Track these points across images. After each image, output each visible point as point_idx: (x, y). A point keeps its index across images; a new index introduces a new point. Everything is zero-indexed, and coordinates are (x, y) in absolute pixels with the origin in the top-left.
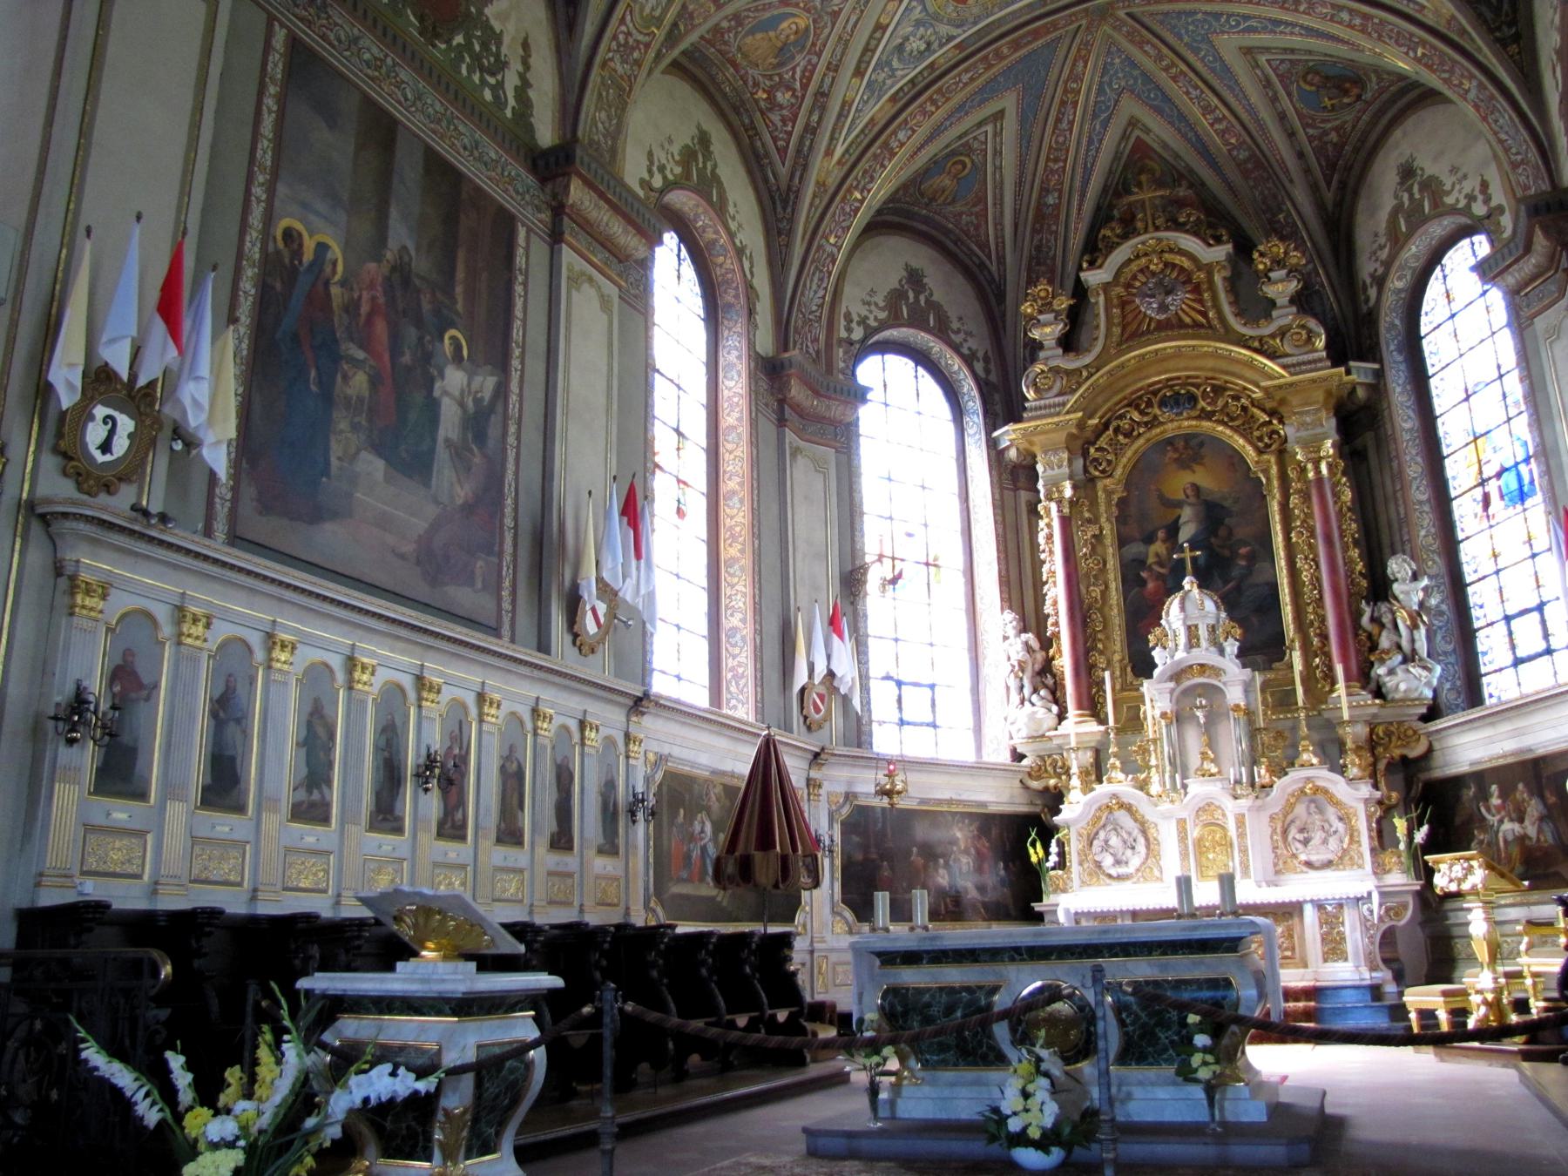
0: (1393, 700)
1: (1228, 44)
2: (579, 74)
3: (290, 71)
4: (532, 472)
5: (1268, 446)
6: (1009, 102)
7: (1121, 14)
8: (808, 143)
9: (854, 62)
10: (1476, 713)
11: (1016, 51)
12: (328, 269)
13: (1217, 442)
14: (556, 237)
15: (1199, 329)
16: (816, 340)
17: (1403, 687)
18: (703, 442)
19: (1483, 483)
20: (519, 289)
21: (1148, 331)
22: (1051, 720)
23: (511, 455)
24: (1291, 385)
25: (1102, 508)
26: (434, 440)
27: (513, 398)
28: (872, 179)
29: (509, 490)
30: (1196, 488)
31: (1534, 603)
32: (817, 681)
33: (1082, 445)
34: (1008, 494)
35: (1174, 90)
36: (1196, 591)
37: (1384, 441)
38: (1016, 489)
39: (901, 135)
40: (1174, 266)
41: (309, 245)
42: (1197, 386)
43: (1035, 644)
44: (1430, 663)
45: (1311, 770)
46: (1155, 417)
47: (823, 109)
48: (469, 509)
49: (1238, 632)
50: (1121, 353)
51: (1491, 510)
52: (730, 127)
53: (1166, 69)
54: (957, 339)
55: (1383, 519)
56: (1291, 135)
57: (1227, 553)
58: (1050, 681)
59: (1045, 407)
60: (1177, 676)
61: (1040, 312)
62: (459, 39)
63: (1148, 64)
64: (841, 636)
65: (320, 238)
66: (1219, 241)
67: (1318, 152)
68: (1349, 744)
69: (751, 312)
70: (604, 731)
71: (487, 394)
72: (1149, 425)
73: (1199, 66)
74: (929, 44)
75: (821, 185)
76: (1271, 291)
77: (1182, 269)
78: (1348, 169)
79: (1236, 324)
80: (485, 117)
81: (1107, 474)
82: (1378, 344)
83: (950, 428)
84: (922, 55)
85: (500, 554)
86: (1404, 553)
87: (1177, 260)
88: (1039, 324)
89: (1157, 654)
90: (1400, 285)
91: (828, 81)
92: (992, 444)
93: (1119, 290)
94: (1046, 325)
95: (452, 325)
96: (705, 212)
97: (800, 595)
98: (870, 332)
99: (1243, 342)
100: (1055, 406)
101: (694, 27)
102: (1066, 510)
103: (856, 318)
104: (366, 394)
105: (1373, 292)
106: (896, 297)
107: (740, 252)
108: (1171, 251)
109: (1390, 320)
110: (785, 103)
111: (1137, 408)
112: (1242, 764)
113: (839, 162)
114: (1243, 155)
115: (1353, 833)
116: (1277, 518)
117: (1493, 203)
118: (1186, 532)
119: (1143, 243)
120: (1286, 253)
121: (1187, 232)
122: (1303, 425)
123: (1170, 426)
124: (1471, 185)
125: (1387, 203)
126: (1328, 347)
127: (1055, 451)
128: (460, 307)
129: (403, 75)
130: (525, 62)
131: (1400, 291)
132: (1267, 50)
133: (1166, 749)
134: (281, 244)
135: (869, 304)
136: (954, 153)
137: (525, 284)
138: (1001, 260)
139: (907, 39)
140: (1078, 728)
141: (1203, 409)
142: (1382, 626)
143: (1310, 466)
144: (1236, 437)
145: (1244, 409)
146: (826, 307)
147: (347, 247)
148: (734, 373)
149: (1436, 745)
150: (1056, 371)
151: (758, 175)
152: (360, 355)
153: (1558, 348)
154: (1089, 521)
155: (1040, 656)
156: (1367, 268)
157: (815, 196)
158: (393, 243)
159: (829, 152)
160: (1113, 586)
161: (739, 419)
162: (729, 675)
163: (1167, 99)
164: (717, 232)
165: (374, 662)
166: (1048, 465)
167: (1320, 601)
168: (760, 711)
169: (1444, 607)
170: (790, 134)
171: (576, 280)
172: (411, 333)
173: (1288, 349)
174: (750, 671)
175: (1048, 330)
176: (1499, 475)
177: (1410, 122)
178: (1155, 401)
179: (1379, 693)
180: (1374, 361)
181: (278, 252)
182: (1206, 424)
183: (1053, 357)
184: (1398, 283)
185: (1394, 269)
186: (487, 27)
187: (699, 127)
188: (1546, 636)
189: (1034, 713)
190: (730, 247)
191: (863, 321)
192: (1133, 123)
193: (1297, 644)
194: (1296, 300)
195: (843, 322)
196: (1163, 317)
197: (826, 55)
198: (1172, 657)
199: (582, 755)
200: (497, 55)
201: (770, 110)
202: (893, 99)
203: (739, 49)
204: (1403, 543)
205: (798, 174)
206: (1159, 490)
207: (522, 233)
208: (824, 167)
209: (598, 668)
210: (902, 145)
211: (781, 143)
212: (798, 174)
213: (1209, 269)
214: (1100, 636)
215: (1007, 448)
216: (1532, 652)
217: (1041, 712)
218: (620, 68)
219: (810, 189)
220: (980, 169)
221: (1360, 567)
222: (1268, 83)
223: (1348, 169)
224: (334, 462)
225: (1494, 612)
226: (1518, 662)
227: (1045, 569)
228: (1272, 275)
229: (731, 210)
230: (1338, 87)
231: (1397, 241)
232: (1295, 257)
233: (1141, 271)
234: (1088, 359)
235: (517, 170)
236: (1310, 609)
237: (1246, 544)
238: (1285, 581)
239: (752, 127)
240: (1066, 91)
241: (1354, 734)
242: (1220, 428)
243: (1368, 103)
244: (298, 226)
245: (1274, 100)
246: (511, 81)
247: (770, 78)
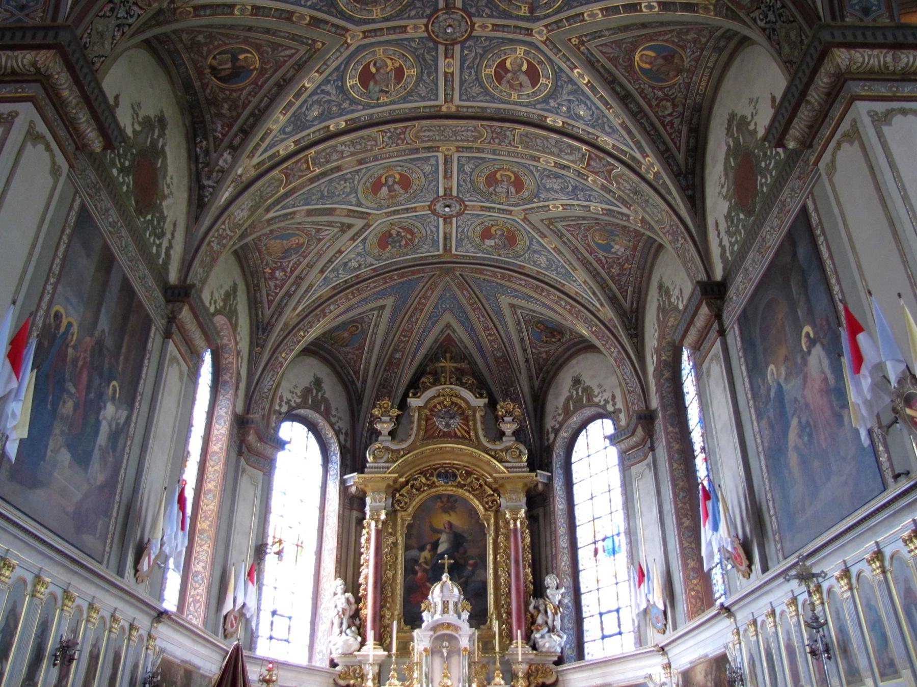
0: (541, 652)
1: (505, 301)
2: (196, 243)
3: (77, 223)
4: (132, 472)
5: (490, 507)
6: (389, 302)
7: (457, 274)
8: (285, 301)
9: (321, 267)
10: (581, 663)
11: (401, 278)
12: (70, 337)
13: (465, 501)
14: (167, 335)
15: (463, 439)
16: (263, 409)
17: (547, 645)
18: (198, 459)
19: (595, 543)
20: (146, 361)
21: (438, 436)
22: (357, 646)
23: (126, 457)
24: (508, 478)
25: (399, 528)
26: (94, 447)
27: (132, 425)
28: (311, 327)
29: (121, 478)
30: (451, 525)
31: (615, 608)
32: (237, 609)
33: (393, 490)
34: (347, 512)
35: (472, 315)
36: (449, 582)
37: (549, 514)
38: (351, 509)
39: (332, 307)
40: (457, 404)
41: (65, 322)
42: (458, 470)
43: (352, 600)
44: (561, 633)
46: (434, 482)
47: (299, 285)
48: (102, 488)
49: (469, 607)
50: (422, 446)
51: (598, 556)
52: (247, 285)
53: (471, 305)
54: (333, 420)
55: (543, 556)
56: (525, 350)
57: (462, 562)
58: (357, 622)
59: (378, 468)
60: (434, 628)
61: (382, 415)
62: (149, 217)
63: (464, 301)
64: (253, 583)
65: (70, 319)
66: (481, 396)
68: (520, 674)
69: (237, 388)
70: (141, 631)
71: (122, 421)
72: (431, 486)
73: (487, 307)
74: (360, 265)
75: (286, 324)
76: (503, 427)
77: (460, 407)
78: (548, 372)
79: (484, 440)
80: (150, 260)
82: (551, 462)
83: (320, 470)
84: (355, 269)
85: (110, 517)
86: (553, 573)
87: (459, 401)
88: (381, 422)
89: (425, 615)
90: (565, 435)
91: (305, 272)
92: (343, 482)
93: (426, 411)
94: (385, 422)
95: (115, 379)
96: (227, 328)
97: (234, 557)
98: (291, 409)
100: (383, 468)
101: (254, 232)
102: (380, 526)
103: (285, 400)
104: (71, 413)
105: (552, 436)
106: (307, 391)
107: (238, 353)
108: (456, 396)
110: (279, 278)
111: (425, 476)
112: (464, 681)
113: (298, 315)
114: (499, 354)
116: (491, 546)
117: (617, 407)
118: (442, 548)
119: (443, 389)
120: (514, 409)
121: (466, 388)
122: (511, 499)
123: (441, 488)
125: (565, 394)
126: (528, 460)
127: (379, 492)
128: (120, 369)
129: (123, 233)
130: (173, 235)
131: (565, 438)
132: (522, 308)
133: (424, 668)
134: (52, 320)
135: (293, 393)
136: (354, 321)
137: (149, 359)
138: (365, 381)
139: (350, 260)
140: (372, 651)
141: (459, 482)
142: (539, 611)
143: (512, 522)
144: (475, 500)
145: (481, 485)
146: (272, 391)
147: (80, 326)
148: (222, 421)
149: (560, 678)
150: (387, 449)
151: (254, 311)
152: (73, 390)
153: (641, 483)
154: (391, 534)
155: (354, 607)
156: (550, 423)
157: (281, 330)
158: (99, 328)
159: (295, 309)
160: (399, 572)
161: (221, 449)
162: (191, 600)
163: (467, 318)
164: (229, 340)
165: (49, 580)
166: (374, 499)
168: (205, 624)
169: (570, 604)
170: (277, 294)
171: (174, 360)
172: (97, 381)
173: (508, 458)
174: (203, 599)
175: (385, 425)
176: (604, 540)
177: (581, 357)
178: (435, 473)
179: (534, 647)
180: (548, 471)
181: (50, 324)
182: (461, 490)
183: (386, 441)
184: (565, 434)
185: (565, 426)
186: (162, 213)
187: (234, 281)
188: (619, 626)
189: (348, 640)
190: (234, 350)
191: (288, 402)
192: (448, 326)
193: (494, 617)
194: (515, 433)
195: (278, 401)
196: (446, 430)
197: (309, 258)
198: (432, 617)
199: (128, 646)
200: (162, 228)
201: (270, 279)
202: (334, 288)
203: (265, 245)
204: (552, 568)
205: (276, 316)
206: (430, 523)
207: (153, 328)
208: (290, 315)
209: (141, 591)
210: (331, 312)
211: (270, 298)
212: (276, 316)
213: (474, 409)
214: (389, 600)
215: (351, 486)
216: (611, 633)
217: (351, 640)
218: (215, 246)
219: (280, 325)
220: (365, 332)
221: (530, 578)
222: (519, 323)
223: (548, 372)
224: (49, 453)
225: (595, 610)
226: (604, 637)
227: (363, 557)
228: (505, 419)
229: (239, 329)
230: (551, 333)
231: (568, 414)
232: (518, 412)
233: (439, 403)
235: (158, 294)
236: (503, 598)
237: (472, 558)
238: (492, 581)
239: (257, 287)
240: (419, 303)
242: (467, 494)
243: (563, 344)
244: (62, 311)
245: (520, 331)
246: (165, 244)
247: (276, 263)
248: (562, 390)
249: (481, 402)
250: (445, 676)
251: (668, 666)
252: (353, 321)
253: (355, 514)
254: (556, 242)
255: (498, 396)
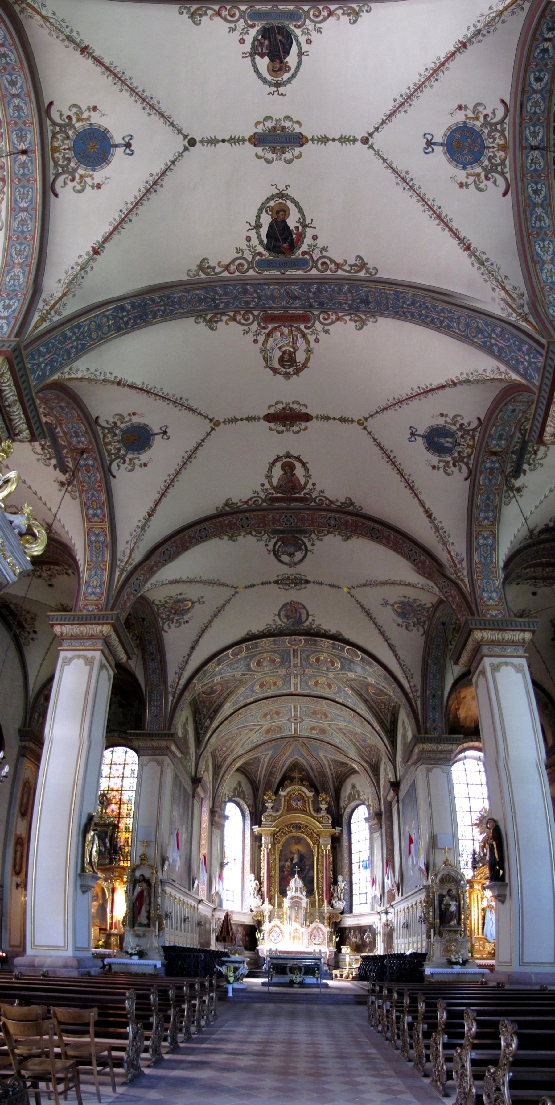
15: (303, 811)
30: (298, 850)
33: (274, 835)
45: (317, 924)
60: (292, 898)
67: (336, 774)
72: (290, 832)
76: (322, 806)
81: (279, 843)
89: (288, 892)
92: (252, 829)
99: (314, 818)
109: (345, 817)
115: (324, 938)
118: (295, 861)
124: (365, 797)
138: (260, 781)
140: (267, 907)
150: (271, 815)
166: (266, 839)
167: (323, 883)
179: (332, 907)
184: (348, 810)
194: (327, 809)
213: (308, 797)
231: (350, 802)
232: (328, 799)
234: (278, 814)
241: (327, 915)
248: (346, 791)
249: (311, 794)
250: (296, 918)
251: (380, 920)
252: (255, 758)
253: (258, 844)
254: (343, 736)
255: (320, 790)
